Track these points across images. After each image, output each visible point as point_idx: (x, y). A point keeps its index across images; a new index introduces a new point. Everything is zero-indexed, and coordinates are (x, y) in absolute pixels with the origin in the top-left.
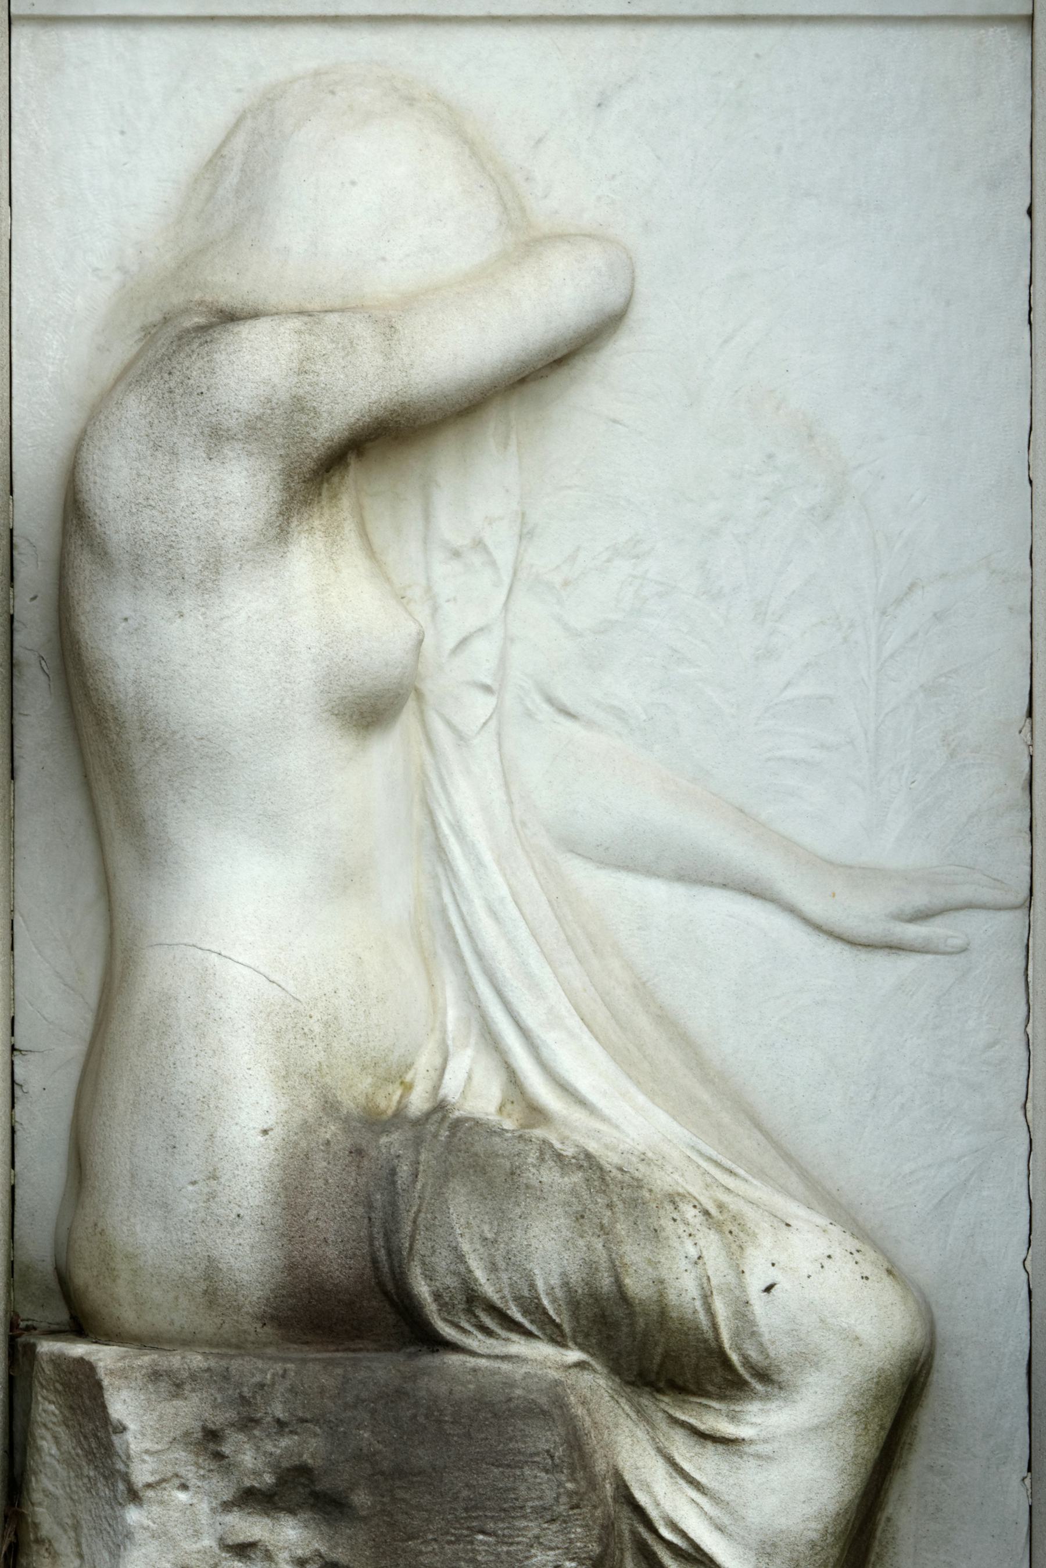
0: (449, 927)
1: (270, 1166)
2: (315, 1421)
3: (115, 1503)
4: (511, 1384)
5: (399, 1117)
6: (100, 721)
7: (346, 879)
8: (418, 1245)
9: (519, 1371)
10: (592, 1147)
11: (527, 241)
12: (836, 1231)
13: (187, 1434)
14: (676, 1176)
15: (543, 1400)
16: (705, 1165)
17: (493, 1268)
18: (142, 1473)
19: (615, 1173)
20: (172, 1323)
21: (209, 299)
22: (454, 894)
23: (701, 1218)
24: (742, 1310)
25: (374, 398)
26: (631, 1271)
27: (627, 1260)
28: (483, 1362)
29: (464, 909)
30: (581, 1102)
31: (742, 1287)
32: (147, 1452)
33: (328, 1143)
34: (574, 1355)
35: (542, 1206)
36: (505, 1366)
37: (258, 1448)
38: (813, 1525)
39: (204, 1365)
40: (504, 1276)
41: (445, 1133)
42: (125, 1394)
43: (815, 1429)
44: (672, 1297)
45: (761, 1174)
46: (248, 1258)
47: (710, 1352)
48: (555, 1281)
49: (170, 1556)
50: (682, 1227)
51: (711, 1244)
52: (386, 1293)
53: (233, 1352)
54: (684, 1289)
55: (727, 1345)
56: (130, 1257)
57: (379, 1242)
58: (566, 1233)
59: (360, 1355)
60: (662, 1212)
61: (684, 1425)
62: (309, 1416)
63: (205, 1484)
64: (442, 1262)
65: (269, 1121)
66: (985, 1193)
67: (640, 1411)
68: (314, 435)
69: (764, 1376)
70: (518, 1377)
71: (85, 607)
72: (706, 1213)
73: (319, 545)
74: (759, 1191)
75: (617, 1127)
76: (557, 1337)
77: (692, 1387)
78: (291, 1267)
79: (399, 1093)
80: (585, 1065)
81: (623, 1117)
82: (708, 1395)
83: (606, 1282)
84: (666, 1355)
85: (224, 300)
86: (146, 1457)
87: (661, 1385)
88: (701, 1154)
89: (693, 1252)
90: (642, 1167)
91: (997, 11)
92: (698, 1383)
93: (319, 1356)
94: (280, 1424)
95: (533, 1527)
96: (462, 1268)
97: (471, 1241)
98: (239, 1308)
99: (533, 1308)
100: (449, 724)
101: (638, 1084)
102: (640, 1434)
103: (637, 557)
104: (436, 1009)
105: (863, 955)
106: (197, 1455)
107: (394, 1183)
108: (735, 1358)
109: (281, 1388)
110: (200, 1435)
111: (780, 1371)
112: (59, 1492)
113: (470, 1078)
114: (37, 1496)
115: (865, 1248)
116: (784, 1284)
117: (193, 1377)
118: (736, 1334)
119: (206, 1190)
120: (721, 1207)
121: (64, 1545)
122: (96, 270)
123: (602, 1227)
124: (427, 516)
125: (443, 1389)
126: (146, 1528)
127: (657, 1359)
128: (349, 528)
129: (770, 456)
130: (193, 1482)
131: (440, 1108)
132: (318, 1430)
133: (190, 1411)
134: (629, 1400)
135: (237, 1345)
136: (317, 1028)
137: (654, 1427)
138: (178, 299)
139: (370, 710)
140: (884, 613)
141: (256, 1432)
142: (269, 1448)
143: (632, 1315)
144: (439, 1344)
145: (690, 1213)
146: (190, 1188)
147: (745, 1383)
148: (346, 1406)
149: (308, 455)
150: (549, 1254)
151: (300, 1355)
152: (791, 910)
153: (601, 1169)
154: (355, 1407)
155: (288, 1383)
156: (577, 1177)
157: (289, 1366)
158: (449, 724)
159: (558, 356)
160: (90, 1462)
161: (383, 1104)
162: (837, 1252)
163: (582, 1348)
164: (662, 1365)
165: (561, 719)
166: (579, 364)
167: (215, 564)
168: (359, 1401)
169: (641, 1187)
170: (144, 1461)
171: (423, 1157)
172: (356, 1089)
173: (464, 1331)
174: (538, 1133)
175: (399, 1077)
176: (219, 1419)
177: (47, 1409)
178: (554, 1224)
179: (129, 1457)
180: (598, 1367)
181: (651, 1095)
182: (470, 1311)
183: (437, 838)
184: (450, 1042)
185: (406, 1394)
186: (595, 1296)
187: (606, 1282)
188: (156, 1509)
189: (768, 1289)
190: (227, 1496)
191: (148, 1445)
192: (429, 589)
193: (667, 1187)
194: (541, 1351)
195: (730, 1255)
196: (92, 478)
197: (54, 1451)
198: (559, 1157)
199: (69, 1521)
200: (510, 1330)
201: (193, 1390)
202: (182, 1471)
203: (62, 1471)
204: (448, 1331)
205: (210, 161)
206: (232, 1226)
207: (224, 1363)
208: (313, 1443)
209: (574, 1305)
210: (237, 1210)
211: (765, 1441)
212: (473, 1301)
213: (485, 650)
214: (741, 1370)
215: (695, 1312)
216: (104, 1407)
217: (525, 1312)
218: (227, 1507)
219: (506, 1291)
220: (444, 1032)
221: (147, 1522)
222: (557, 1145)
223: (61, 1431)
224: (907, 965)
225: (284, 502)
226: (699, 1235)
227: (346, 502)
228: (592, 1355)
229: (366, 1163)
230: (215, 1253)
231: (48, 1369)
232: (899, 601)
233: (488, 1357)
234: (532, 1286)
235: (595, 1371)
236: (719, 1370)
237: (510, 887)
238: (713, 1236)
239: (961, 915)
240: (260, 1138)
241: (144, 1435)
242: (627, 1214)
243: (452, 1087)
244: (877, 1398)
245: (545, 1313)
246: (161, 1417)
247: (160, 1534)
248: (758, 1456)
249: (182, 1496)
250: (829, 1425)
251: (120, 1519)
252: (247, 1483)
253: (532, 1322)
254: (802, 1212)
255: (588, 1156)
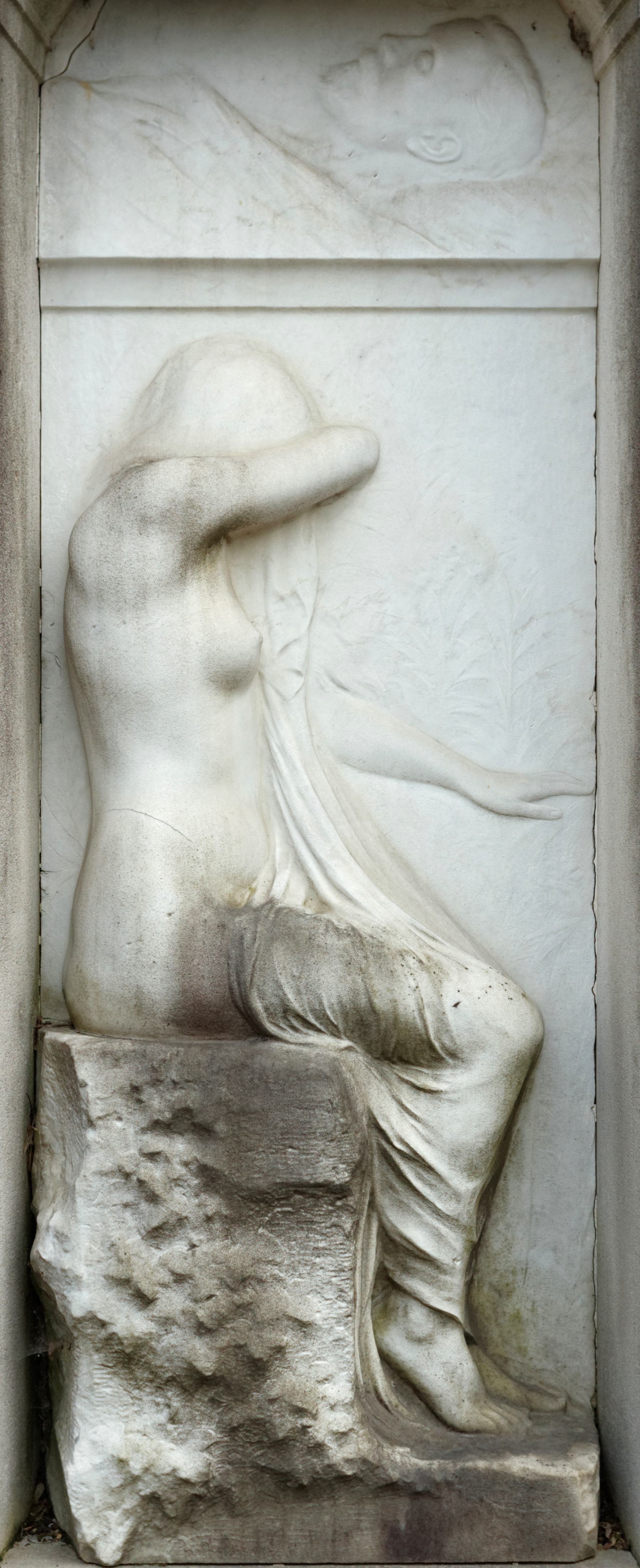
0: (277, 803)
1: (172, 933)
2: (194, 1081)
3: (81, 1126)
4: (309, 1061)
5: (248, 907)
6: (82, 686)
7: (220, 774)
8: (255, 980)
9: (313, 1052)
10: (356, 924)
11: (319, 426)
12: (493, 972)
13: (121, 1088)
14: (403, 941)
15: (327, 1070)
16: (419, 934)
17: (298, 993)
18: (96, 1110)
19: (368, 938)
20: (118, 1022)
21: (145, 455)
22: (280, 785)
23: (417, 964)
24: (441, 1018)
25: (234, 503)
26: (378, 995)
27: (375, 988)
28: (292, 1047)
29: (285, 793)
30: (349, 899)
31: (441, 1004)
32: (98, 1098)
33: (206, 921)
34: (345, 1043)
35: (327, 957)
36: (305, 1050)
37: (162, 1097)
38: (481, 1140)
39: (132, 1048)
40: (305, 997)
41: (272, 916)
42: (87, 1065)
43: (482, 1085)
44: (401, 1010)
45: (450, 940)
46: (159, 986)
47: (423, 1041)
48: (334, 1000)
49: (111, 1159)
50: (407, 970)
51: (423, 980)
52: (237, 1007)
53: (152, 1040)
54: (408, 1005)
55: (432, 1037)
56: (95, 985)
57: (233, 978)
58: (340, 973)
59: (223, 1042)
60: (395, 961)
61: (407, 1082)
62: (191, 1079)
63: (132, 1117)
64: (269, 989)
65: (172, 908)
66: (571, 951)
67: (383, 1075)
68: (200, 522)
69: (453, 1055)
70: (313, 1056)
71: (73, 621)
72: (420, 962)
73: (204, 587)
74: (449, 949)
75: (370, 913)
76: (335, 1032)
77: (412, 1061)
78: (184, 992)
79: (248, 894)
80: (353, 880)
81: (374, 908)
82: (420, 1065)
83: (363, 1001)
84: (398, 1043)
85: (153, 455)
86: (98, 1101)
87: (395, 1059)
88: (417, 928)
89: (413, 984)
90: (384, 935)
91: (577, 305)
92: (415, 1058)
93: (200, 1042)
94: (175, 1083)
95: (320, 1145)
96: (281, 993)
97: (286, 977)
98: (155, 1015)
99: (322, 1016)
100: (278, 692)
101: (381, 889)
102: (383, 1087)
103: (381, 602)
104: (270, 848)
105: (505, 820)
106: (127, 1100)
107: (242, 944)
108: (437, 1044)
109: (175, 1062)
110: (129, 1089)
111: (463, 1052)
112: (54, 1118)
113: (288, 886)
114: (43, 1120)
115: (510, 982)
116: (465, 1002)
117: (125, 1055)
118: (438, 1031)
119: (136, 947)
120: (429, 958)
121: (57, 1148)
122: (87, 446)
123: (361, 969)
124: (266, 577)
125: (269, 1063)
126: (98, 1143)
127: (393, 1045)
128: (221, 580)
129: (454, 547)
130: (125, 1116)
131: (271, 902)
132: (196, 1087)
133: (123, 1075)
134: (376, 1068)
135: (153, 1036)
136: (201, 856)
137: (390, 1084)
138: (129, 457)
139: (233, 680)
140: (516, 633)
141: (161, 1088)
142: (168, 1097)
143: (378, 1020)
144: (267, 1036)
145: (411, 961)
146: (127, 946)
147: (443, 1059)
148: (213, 1073)
149: (197, 534)
150: (331, 985)
151: (190, 1042)
152: (466, 796)
153: (361, 936)
154: (218, 1073)
155: (179, 1059)
156: (347, 941)
157: (181, 1049)
158: (278, 692)
159: (338, 490)
160: (70, 1102)
161: (239, 900)
162: (494, 984)
163: (349, 1038)
164: (395, 1048)
165: (339, 691)
166: (349, 496)
167: (143, 594)
168: (220, 1070)
169: (383, 947)
170: (96, 1104)
171: (259, 929)
172: (223, 892)
173: (282, 1029)
174: (326, 916)
175: (248, 885)
176: (139, 1080)
177: (48, 1071)
178: (333, 968)
179: (88, 1101)
180: (359, 1050)
181: (389, 896)
182: (285, 1018)
183: (271, 755)
184: (277, 866)
185: (247, 1066)
186: (357, 1009)
187: (363, 1001)
188: (103, 1131)
189: (456, 1005)
190: (144, 1124)
191: (99, 1094)
192: (267, 618)
193: (398, 947)
194: (325, 1041)
195: (434, 986)
196: (77, 549)
197: (52, 1094)
198: (337, 929)
199: (59, 1134)
200: (309, 1028)
201: (125, 1063)
202: (119, 1110)
203: (56, 1107)
204: (272, 1029)
205: (149, 386)
206: (150, 968)
207: (143, 1047)
208: (193, 1094)
209: (345, 1015)
210: (153, 959)
211: (454, 1092)
212: (287, 1011)
213: (297, 652)
214: (440, 1051)
215: (414, 1018)
216: (75, 1072)
217: (317, 1018)
218: (144, 1130)
219: (306, 1006)
220: (274, 861)
221: (98, 1139)
222: (336, 923)
223: (55, 1083)
224: (528, 826)
225: (183, 560)
226: (417, 974)
227: (220, 565)
228: (356, 1043)
229: (227, 932)
230: (141, 984)
231: (49, 1048)
232: (524, 627)
233: (296, 1044)
234: (321, 1003)
235: (357, 1052)
236: (428, 1051)
237: (311, 781)
238: (424, 975)
239: (558, 799)
240: (167, 918)
241: (97, 1088)
242: (376, 962)
243: (277, 891)
244: (517, 1067)
245: (328, 1019)
246: (107, 1078)
247: (106, 1146)
248: (450, 1101)
249: (119, 1124)
250: (491, 1083)
251: (83, 1136)
252: (156, 1117)
253: (321, 1024)
254: (474, 961)
255: (353, 929)
